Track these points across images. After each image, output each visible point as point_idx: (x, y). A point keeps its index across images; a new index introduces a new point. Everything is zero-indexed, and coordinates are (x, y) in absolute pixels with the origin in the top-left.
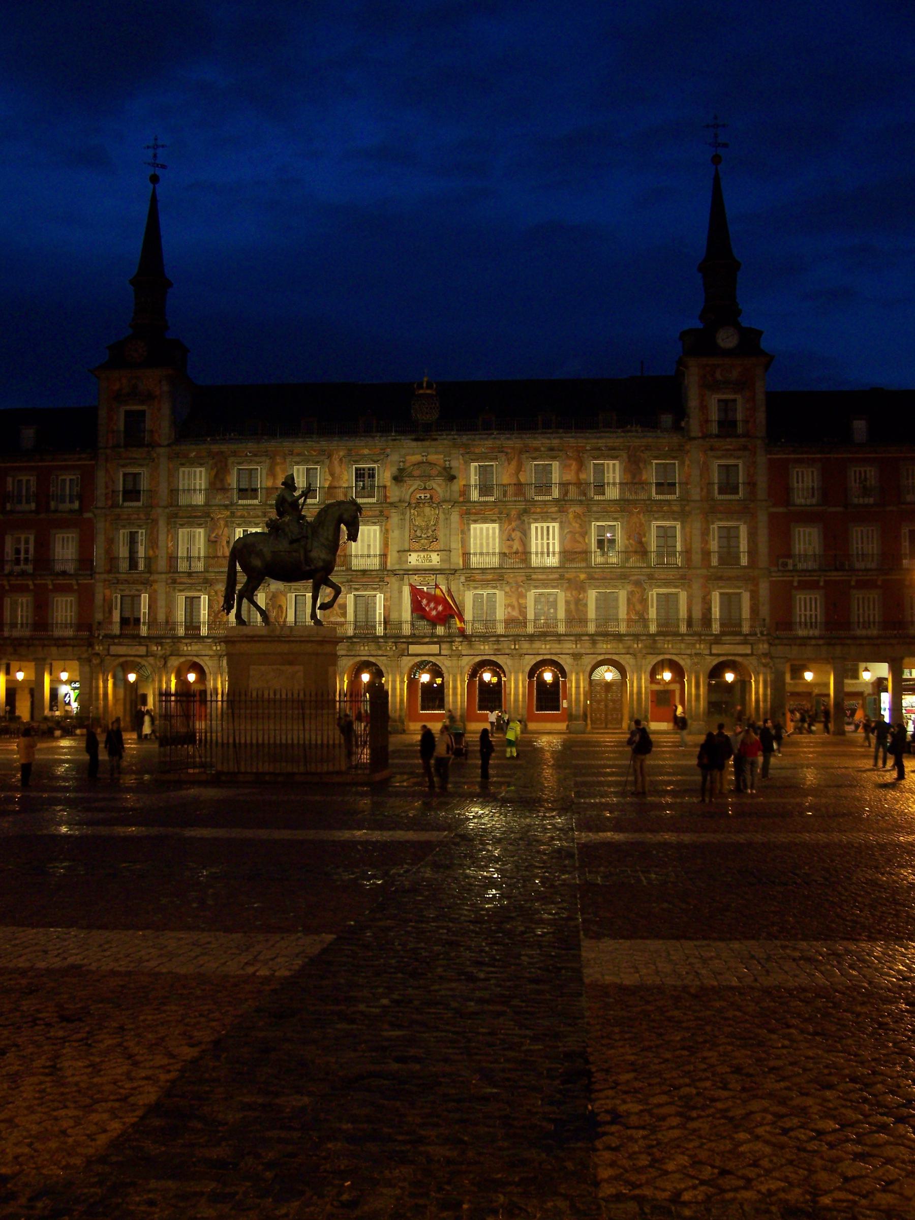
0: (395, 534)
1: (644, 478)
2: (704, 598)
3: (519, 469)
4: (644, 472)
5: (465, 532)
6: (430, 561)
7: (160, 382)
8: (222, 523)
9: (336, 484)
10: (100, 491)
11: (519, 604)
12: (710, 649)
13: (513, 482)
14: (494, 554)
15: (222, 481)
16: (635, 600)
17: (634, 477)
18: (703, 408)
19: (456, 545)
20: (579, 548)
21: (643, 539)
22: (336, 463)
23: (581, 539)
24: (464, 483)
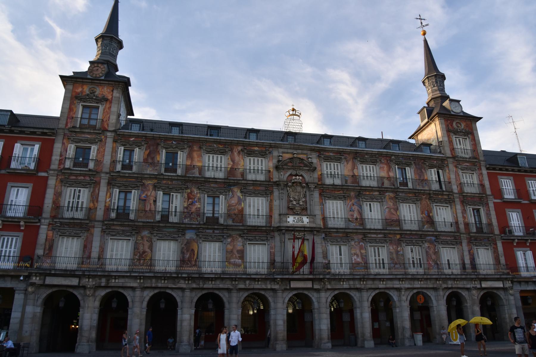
0: (276, 203)
1: (426, 178)
2: (469, 251)
4: (425, 174)
5: (322, 204)
6: (303, 222)
7: (112, 91)
8: (151, 187)
10: (56, 158)
12: (481, 284)
13: (352, 174)
15: (153, 158)
16: (431, 252)
17: (420, 176)
18: (451, 142)
19: (317, 211)
20: (395, 218)
21: (431, 214)
22: (236, 154)
23: (394, 213)
24: (320, 173)
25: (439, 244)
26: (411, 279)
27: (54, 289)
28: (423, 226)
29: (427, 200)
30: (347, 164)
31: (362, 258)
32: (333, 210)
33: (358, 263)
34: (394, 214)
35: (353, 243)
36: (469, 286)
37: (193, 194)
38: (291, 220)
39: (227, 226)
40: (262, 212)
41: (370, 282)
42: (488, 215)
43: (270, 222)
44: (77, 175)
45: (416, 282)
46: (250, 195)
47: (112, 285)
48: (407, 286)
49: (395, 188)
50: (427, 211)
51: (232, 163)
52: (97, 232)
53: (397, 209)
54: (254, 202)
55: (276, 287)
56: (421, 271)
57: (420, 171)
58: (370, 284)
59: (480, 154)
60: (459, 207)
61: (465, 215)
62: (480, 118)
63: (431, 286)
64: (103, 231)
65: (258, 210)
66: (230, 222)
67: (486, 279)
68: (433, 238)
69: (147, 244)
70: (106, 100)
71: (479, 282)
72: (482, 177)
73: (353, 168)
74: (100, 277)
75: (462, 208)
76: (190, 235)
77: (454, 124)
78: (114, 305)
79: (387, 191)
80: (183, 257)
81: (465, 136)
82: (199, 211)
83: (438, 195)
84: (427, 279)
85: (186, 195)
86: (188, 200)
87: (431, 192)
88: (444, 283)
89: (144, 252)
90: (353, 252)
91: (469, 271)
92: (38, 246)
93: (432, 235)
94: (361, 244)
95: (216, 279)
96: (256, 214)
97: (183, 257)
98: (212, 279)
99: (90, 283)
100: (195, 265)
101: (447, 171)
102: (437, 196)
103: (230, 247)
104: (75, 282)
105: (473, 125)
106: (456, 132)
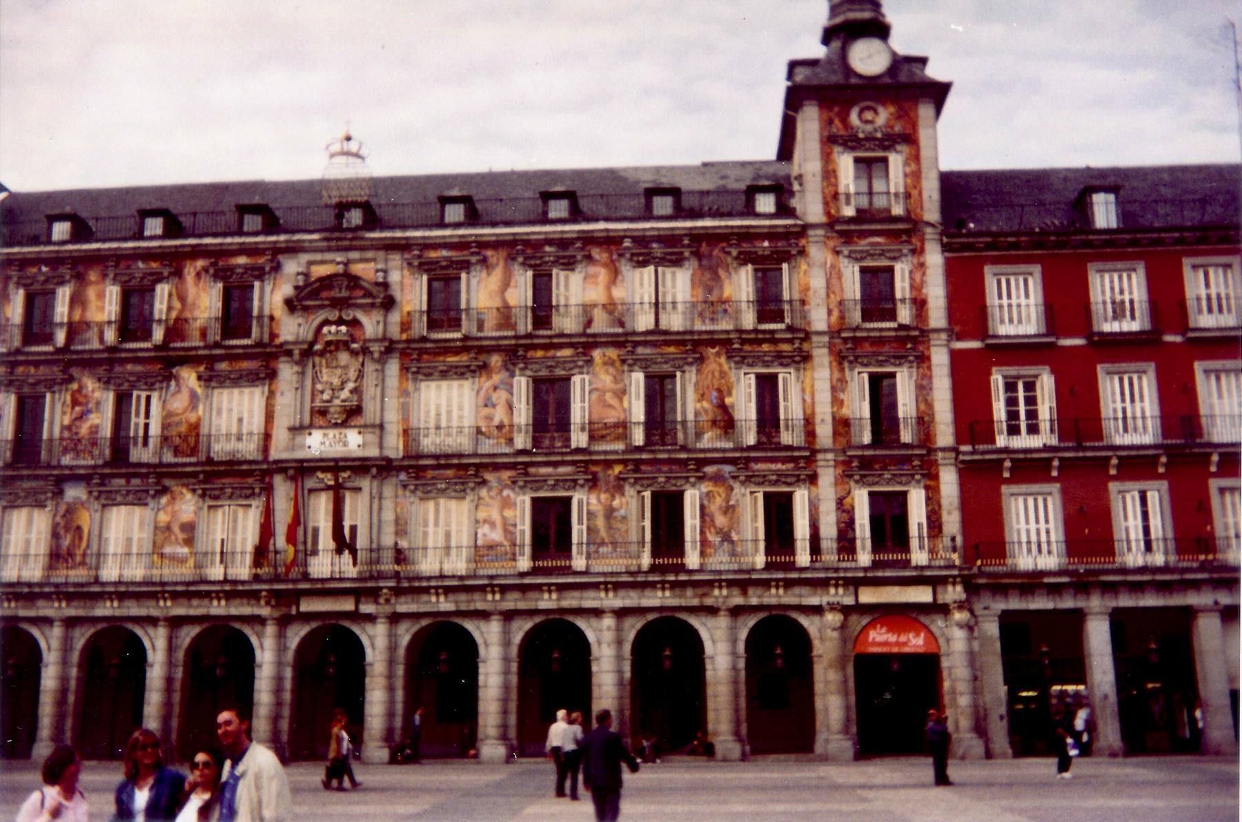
2: (840, 502)
3: (506, 284)
6: (345, 445)
9: (188, 314)
11: (504, 518)
13: (497, 303)
14: (460, 430)
16: (715, 506)
17: (709, 290)
18: (829, 174)
19: (392, 417)
20: (612, 417)
21: (728, 401)
25: (743, 483)
28: (699, 435)
29: (723, 360)
30: (489, 274)
31: (506, 531)
32: (438, 406)
33: (491, 547)
34: (610, 406)
35: (483, 492)
36: (814, 601)
37: (84, 392)
38: (318, 444)
39: (161, 465)
40: (250, 423)
41: (514, 595)
42: (923, 390)
43: (266, 449)
45: (648, 592)
46: (221, 385)
49: (626, 334)
50: (719, 391)
51: (177, 305)
53: (621, 393)
54: (230, 401)
55: (265, 611)
57: (710, 276)
58: (512, 602)
59: (926, 205)
61: (842, 396)
63: (695, 602)
65: (240, 420)
66: (169, 457)
68: (727, 469)
71: (852, 589)
72: (924, 274)
73: (506, 284)
75: (837, 375)
76: (73, 493)
79: (596, 345)
82: (96, 432)
85: (69, 398)
86: (73, 408)
87: (732, 336)
90: (481, 515)
91: (830, 555)
94: (505, 493)
96: (234, 430)
97: (58, 546)
100: (83, 563)
101: (804, 267)
103: (163, 517)
106: (851, 141)
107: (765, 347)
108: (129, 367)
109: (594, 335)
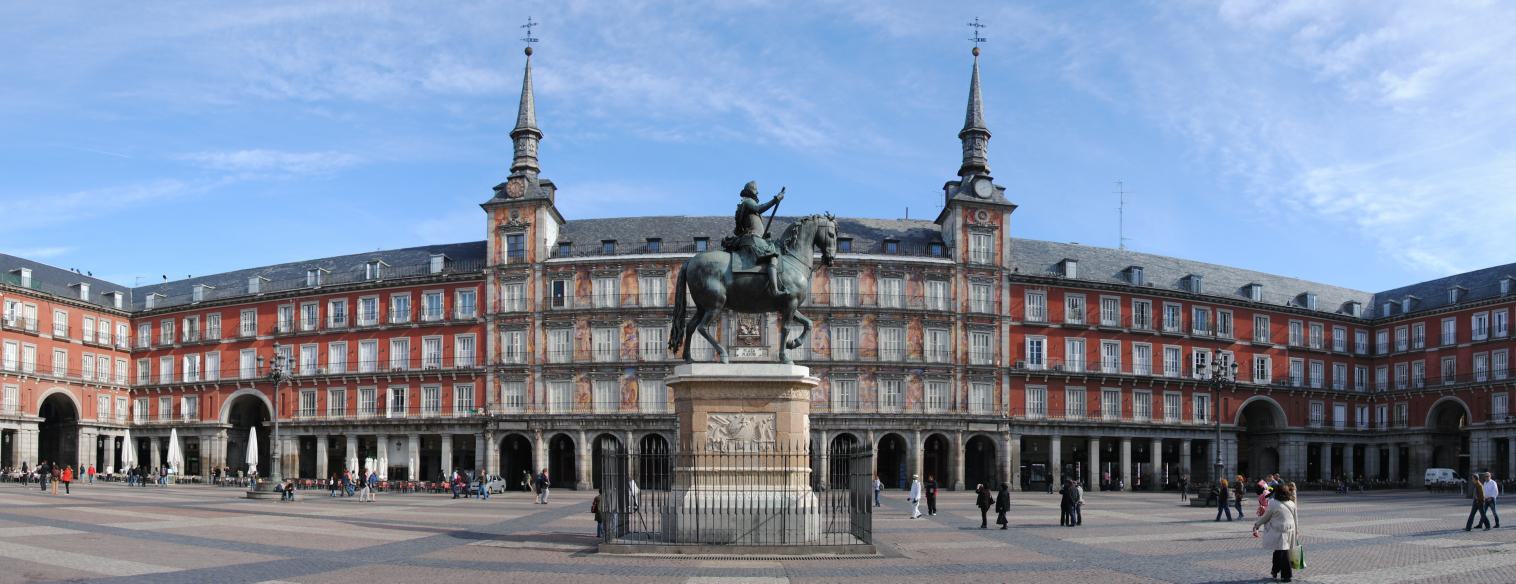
6: (754, 354)
15: (585, 290)
17: (914, 291)
26: (881, 420)
27: (508, 433)
33: (819, 402)
36: (952, 428)
41: (831, 423)
44: (512, 318)
47: (558, 428)
48: (875, 427)
52: (538, 375)
56: (893, 410)
58: (830, 425)
60: (960, 333)
62: (1015, 207)
63: (905, 427)
64: (544, 376)
67: (975, 420)
68: (919, 371)
69: (587, 386)
70: (529, 225)
73: (824, 285)
74: (546, 421)
77: (977, 213)
78: (562, 447)
80: (624, 398)
81: (988, 232)
83: (935, 316)
84: (901, 420)
85: (622, 330)
88: (922, 424)
89: (584, 394)
92: (488, 394)
93: (919, 368)
95: (657, 421)
97: (624, 398)
98: (653, 421)
99: (537, 426)
101: (953, 283)
102: (933, 319)
104: (523, 426)
105: (1005, 216)
106: (976, 228)
107: (937, 318)
108: (651, 316)
109: (865, 309)
